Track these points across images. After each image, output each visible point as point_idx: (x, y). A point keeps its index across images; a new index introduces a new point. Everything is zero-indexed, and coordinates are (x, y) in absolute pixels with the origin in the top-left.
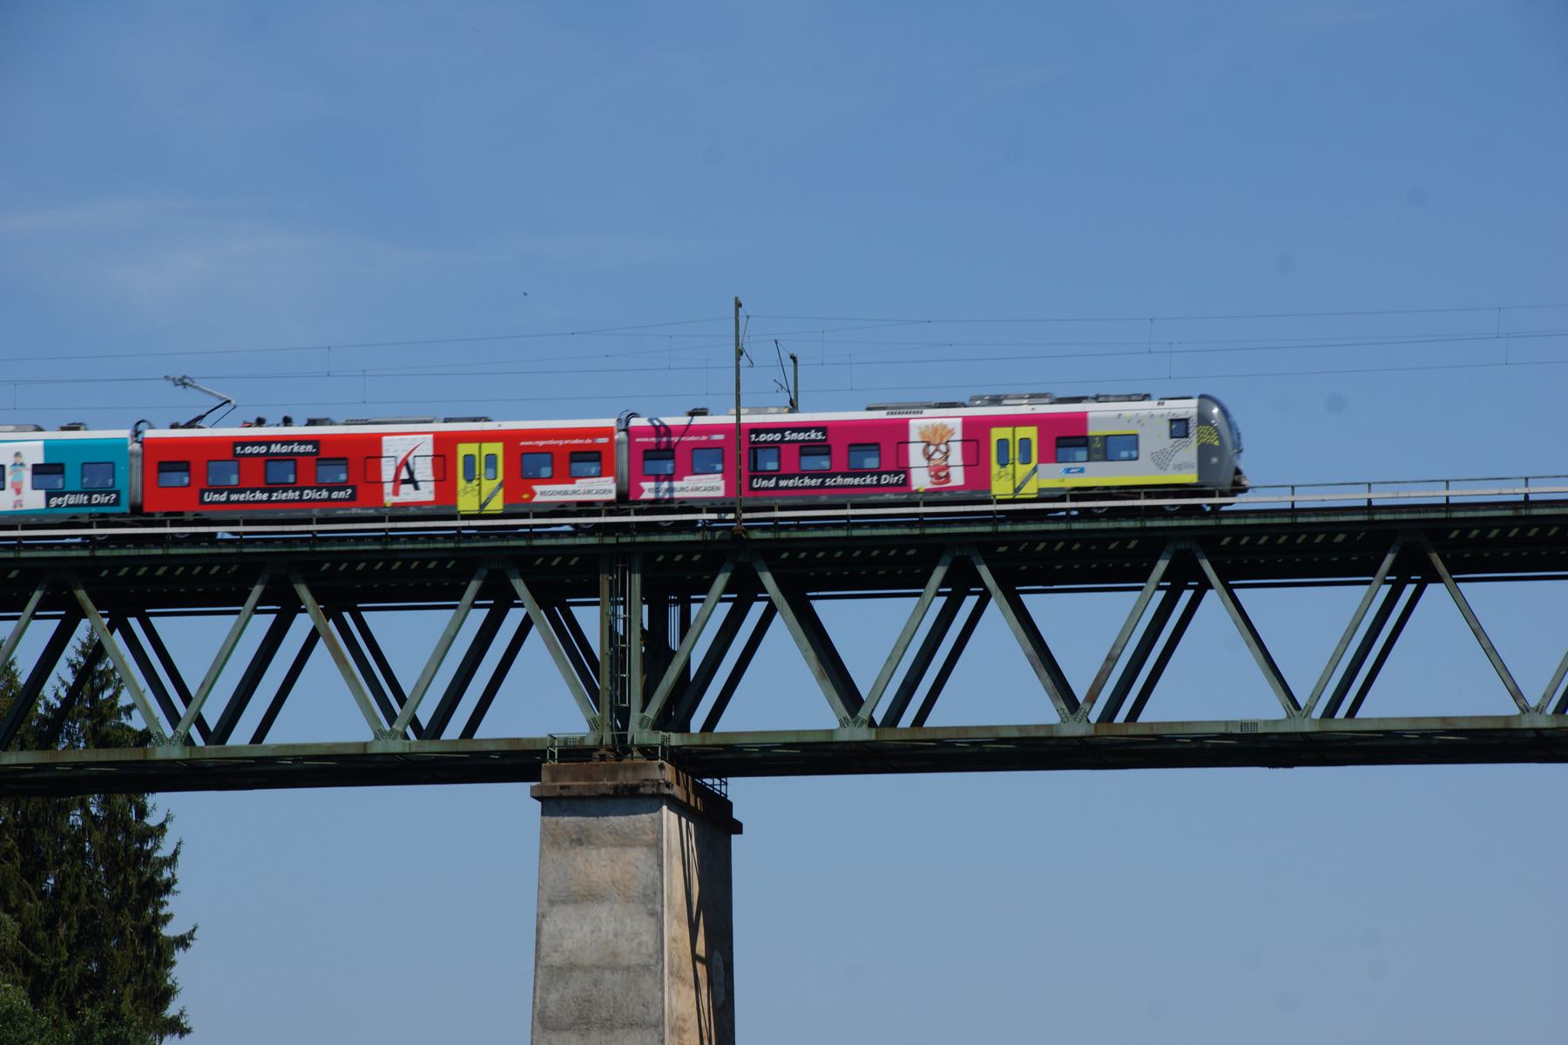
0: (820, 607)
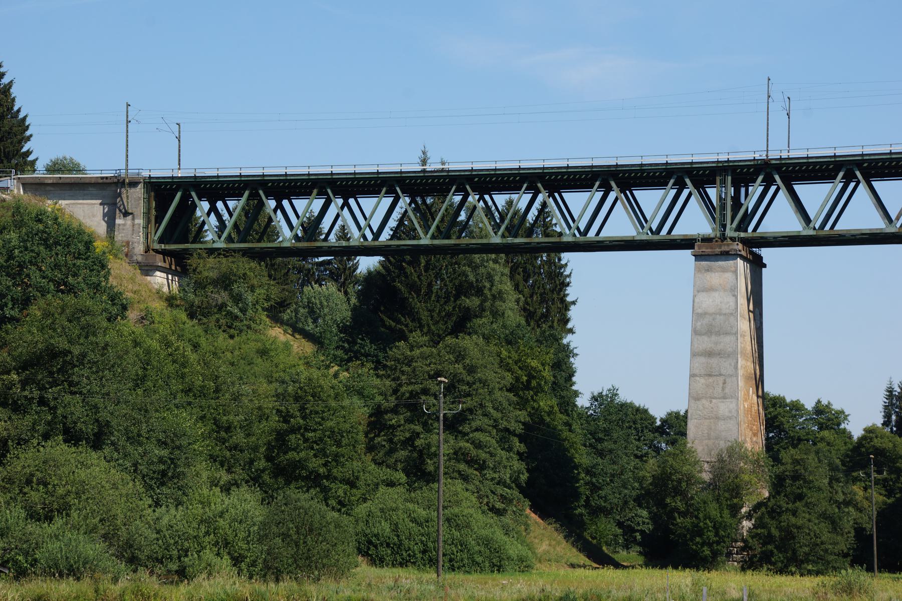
0: (795, 187)
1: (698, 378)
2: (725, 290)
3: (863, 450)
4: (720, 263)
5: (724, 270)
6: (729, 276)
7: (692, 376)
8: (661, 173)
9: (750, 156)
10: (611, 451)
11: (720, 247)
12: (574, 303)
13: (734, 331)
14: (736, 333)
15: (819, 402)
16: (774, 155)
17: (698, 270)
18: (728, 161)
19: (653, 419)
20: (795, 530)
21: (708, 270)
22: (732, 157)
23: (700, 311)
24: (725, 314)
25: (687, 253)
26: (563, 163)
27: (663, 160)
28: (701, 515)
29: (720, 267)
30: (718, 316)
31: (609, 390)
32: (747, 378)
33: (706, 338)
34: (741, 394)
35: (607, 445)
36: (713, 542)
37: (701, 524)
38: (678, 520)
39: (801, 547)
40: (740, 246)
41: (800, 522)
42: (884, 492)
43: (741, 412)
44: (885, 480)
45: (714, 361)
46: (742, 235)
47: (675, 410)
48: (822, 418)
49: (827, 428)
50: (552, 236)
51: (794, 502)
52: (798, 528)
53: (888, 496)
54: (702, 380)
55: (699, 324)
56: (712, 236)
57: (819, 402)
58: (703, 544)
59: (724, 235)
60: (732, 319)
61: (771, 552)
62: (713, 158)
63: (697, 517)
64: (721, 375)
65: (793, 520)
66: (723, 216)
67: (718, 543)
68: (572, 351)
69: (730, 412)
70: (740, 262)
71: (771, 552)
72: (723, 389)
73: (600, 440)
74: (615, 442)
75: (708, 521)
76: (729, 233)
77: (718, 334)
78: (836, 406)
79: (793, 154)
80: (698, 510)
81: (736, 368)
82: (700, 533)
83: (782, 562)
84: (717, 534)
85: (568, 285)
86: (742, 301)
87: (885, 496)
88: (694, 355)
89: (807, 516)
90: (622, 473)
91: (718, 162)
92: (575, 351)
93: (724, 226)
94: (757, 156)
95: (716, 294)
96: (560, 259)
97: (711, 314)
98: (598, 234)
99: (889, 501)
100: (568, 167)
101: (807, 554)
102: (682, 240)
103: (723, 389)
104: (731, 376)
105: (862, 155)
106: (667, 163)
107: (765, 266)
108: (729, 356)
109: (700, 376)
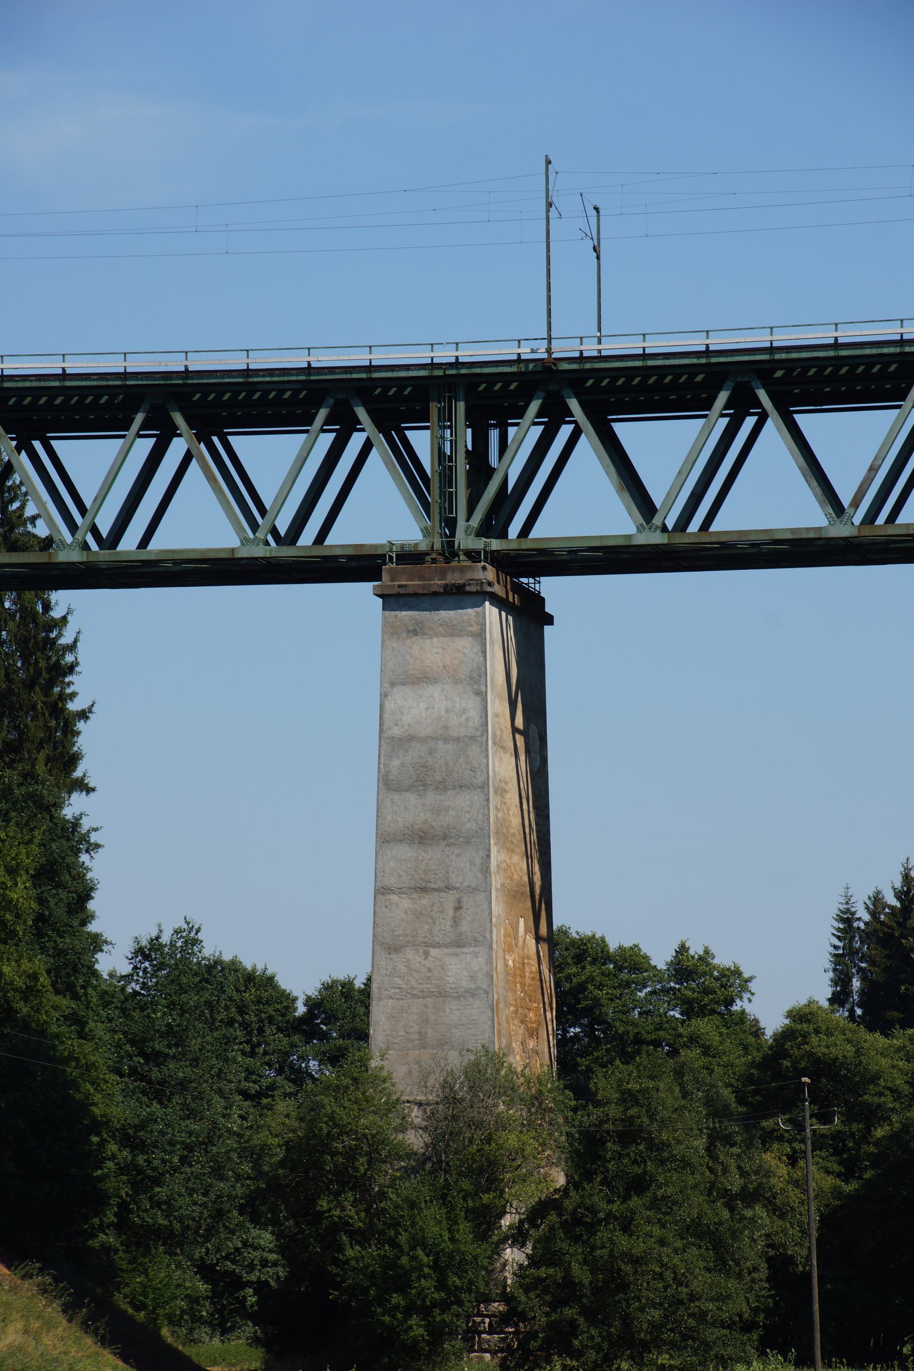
0: (618, 427)
1: (394, 898)
2: (457, 681)
3: (786, 1063)
4: (444, 614)
5: (454, 631)
6: (465, 644)
7: (381, 891)
8: (296, 392)
9: (508, 352)
10: (183, 1085)
11: (443, 575)
12: (84, 715)
13: (480, 780)
14: (485, 786)
15: (683, 949)
16: (564, 349)
17: (390, 631)
18: (457, 364)
19: (288, 1000)
20: (628, 1268)
21: (415, 631)
22: (467, 354)
23: (396, 732)
24: (458, 740)
25: (364, 590)
26: (52, 366)
27: (298, 360)
28: (403, 1238)
29: (444, 623)
30: (440, 744)
31: (177, 932)
32: (512, 896)
33: (412, 798)
34: (498, 935)
35: (177, 1070)
36: (434, 1305)
37: (404, 1260)
38: (350, 1253)
39: (642, 1309)
40: (490, 574)
41: (639, 1248)
42: (836, 1168)
43: (499, 979)
44: (838, 1136)
45: (432, 855)
46: (496, 544)
47: (341, 976)
48: (689, 990)
49: (703, 1011)
50: (24, 548)
51: (626, 1198)
52: (636, 1261)
53: (846, 1177)
54: (405, 903)
55: (396, 763)
56: (423, 547)
57: (683, 949)
58: (408, 1312)
59: (451, 544)
60: (474, 751)
61: (573, 1323)
62: (422, 356)
63: (394, 1244)
64: (449, 888)
65: (624, 1242)
66: (449, 499)
67: (444, 1306)
68: (85, 838)
69: (473, 978)
70: (491, 612)
71: (573, 1323)
72: (456, 922)
73: (157, 1058)
74: (195, 1062)
75: (420, 1253)
76: (465, 540)
77: (442, 787)
78: (722, 959)
79: (610, 347)
80: (396, 1225)
81: (486, 870)
82: (401, 1283)
83: (598, 1348)
84: (442, 1285)
85: (71, 669)
86: (498, 706)
87: (839, 1175)
88: (385, 839)
89: (657, 1231)
90: (209, 1142)
91: (433, 366)
92: (94, 838)
93: (451, 524)
94: (526, 352)
95: (435, 691)
96: (47, 607)
97: (424, 740)
98: (144, 542)
99: (848, 1188)
100: (64, 376)
101: (656, 1327)
102: (351, 558)
103: (456, 922)
104: (474, 890)
105: (772, 350)
106: (309, 369)
107: (549, 620)
108: (468, 842)
109: (401, 891)
